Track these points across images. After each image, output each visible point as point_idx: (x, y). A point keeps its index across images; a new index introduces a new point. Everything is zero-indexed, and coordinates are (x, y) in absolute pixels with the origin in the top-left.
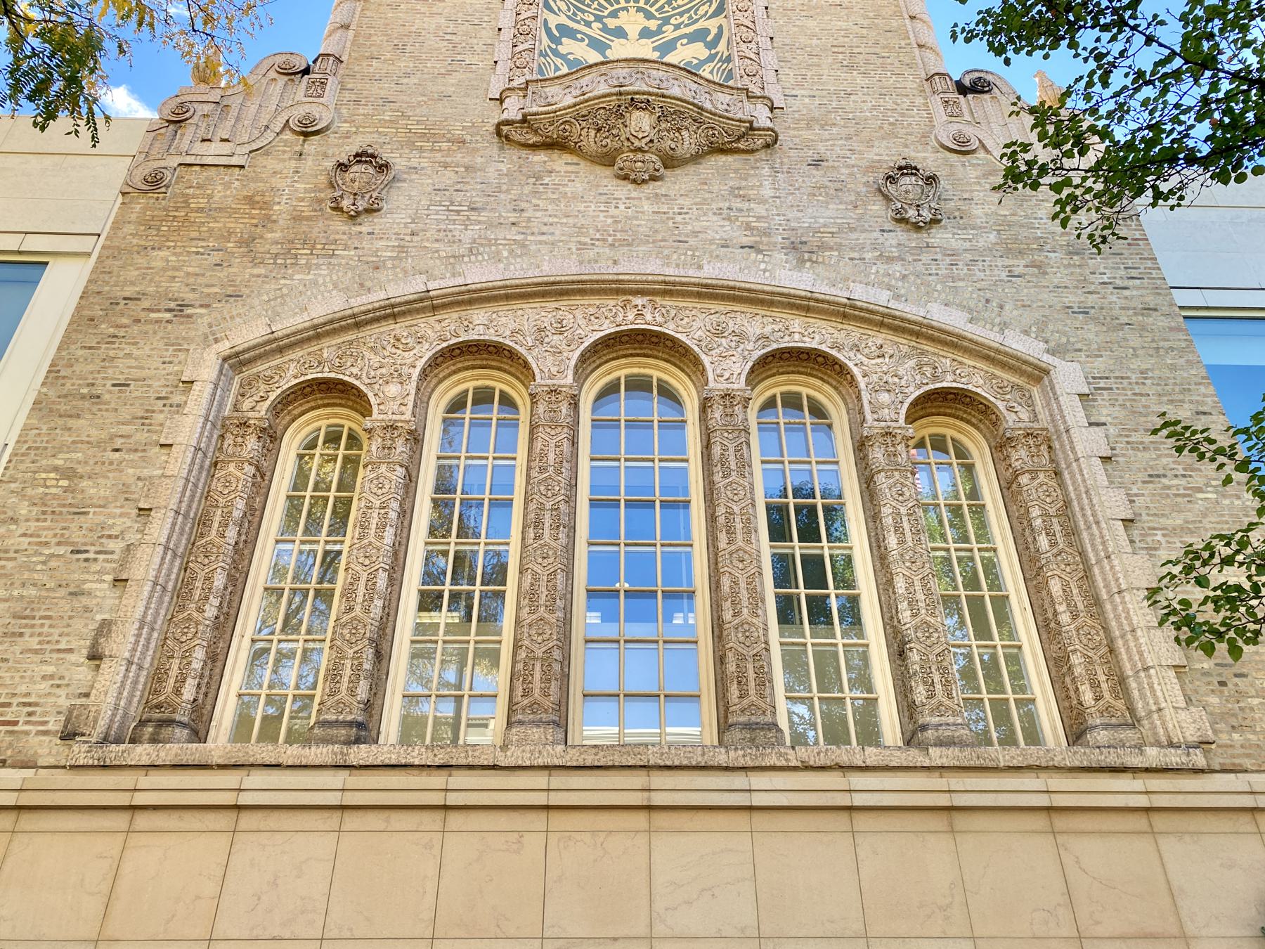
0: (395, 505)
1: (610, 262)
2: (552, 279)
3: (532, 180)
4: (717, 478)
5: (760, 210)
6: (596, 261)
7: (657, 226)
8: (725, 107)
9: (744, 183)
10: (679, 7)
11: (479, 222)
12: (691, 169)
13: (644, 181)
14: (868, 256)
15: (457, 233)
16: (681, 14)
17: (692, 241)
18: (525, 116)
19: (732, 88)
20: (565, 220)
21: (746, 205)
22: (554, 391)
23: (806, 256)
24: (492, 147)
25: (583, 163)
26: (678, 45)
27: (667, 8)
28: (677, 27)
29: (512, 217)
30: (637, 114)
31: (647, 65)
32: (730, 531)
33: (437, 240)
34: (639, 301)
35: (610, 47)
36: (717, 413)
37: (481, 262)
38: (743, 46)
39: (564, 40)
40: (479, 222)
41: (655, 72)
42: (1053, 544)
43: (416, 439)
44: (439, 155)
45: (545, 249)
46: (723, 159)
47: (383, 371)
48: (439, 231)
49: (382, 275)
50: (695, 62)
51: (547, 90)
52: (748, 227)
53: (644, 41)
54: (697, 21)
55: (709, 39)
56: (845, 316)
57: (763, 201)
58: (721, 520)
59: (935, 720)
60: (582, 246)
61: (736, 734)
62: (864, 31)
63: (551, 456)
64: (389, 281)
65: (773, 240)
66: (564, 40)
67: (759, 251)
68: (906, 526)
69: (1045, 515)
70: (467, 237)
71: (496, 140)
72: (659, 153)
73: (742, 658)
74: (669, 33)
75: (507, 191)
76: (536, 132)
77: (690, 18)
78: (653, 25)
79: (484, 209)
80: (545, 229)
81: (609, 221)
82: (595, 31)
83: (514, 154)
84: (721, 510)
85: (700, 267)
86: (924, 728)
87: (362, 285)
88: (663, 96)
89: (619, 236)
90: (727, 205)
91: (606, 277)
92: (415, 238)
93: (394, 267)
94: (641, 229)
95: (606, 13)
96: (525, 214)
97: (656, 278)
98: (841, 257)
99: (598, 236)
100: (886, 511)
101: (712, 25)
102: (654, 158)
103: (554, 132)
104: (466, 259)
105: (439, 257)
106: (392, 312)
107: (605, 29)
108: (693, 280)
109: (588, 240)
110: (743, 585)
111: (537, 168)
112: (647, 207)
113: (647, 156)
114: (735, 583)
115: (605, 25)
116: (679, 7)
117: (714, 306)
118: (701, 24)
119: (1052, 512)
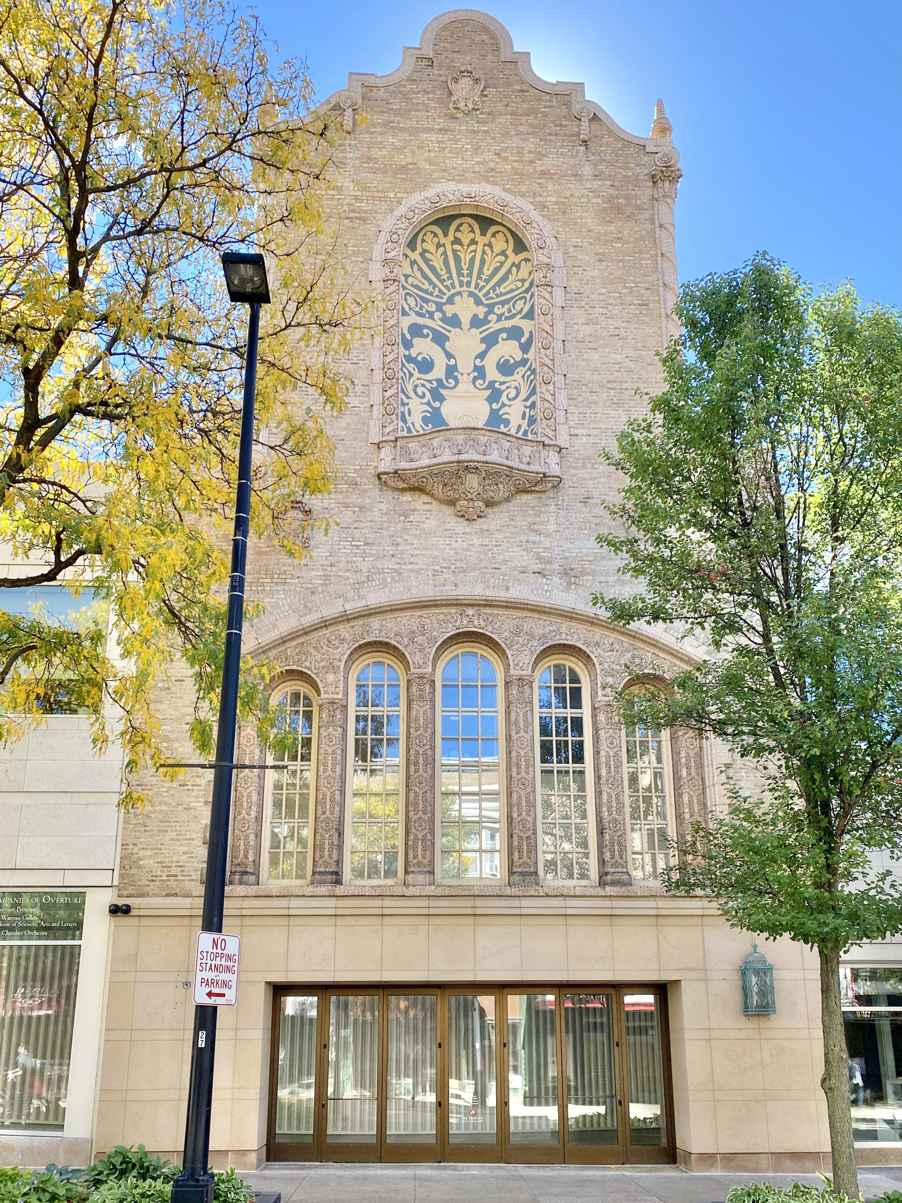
0: (339, 752)
3: (403, 518)
4: (513, 733)
5: (546, 542)
8: (528, 459)
10: (502, 294)
11: (372, 555)
12: (504, 506)
14: (610, 579)
16: (503, 303)
21: (536, 538)
22: (421, 677)
23: (573, 580)
25: (434, 502)
27: (492, 295)
29: (391, 550)
32: (518, 766)
34: (470, 611)
35: (448, 339)
36: (514, 691)
38: (544, 387)
39: (416, 341)
40: (372, 555)
42: (689, 774)
43: (345, 707)
44: (341, 496)
45: (413, 576)
46: (525, 497)
47: (323, 663)
49: (317, 598)
50: (512, 361)
52: (539, 557)
54: (514, 316)
55: (523, 340)
56: (592, 623)
58: (514, 759)
59: (613, 870)
60: (436, 573)
61: (516, 878)
62: (632, 365)
63: (421, 720)
64: (322, 603)
66: (416, 341)
67: (544, 576)
68: (612, 763)
69: (688, 756)
70: (365, 567)
72: (483, 500)
73: (521, 838)
74: (494, 326)
77: (509, 310)
78: (481, 311)
80: (412, 559)
81: (452, 552)
82: (436, 324)
83: (389, 495)
84: (514, 754)
85: (507, 589)
86: (607, 874)
87: (306, 606)
92: (334, 569)
93: (323, 592)
94: (472, 559)
100: (603, 753)
101: (526, 326)
102: (481, 504)
106: (325, 624)
107: (444, 319)
109: (438, 568)
110: (523, 798)
112: (476, 541)
114: (519, 797)
115: (444, 313)
116: (502, 294)
117: (515, 613)
118: (517, 322)
119: (692, 755)
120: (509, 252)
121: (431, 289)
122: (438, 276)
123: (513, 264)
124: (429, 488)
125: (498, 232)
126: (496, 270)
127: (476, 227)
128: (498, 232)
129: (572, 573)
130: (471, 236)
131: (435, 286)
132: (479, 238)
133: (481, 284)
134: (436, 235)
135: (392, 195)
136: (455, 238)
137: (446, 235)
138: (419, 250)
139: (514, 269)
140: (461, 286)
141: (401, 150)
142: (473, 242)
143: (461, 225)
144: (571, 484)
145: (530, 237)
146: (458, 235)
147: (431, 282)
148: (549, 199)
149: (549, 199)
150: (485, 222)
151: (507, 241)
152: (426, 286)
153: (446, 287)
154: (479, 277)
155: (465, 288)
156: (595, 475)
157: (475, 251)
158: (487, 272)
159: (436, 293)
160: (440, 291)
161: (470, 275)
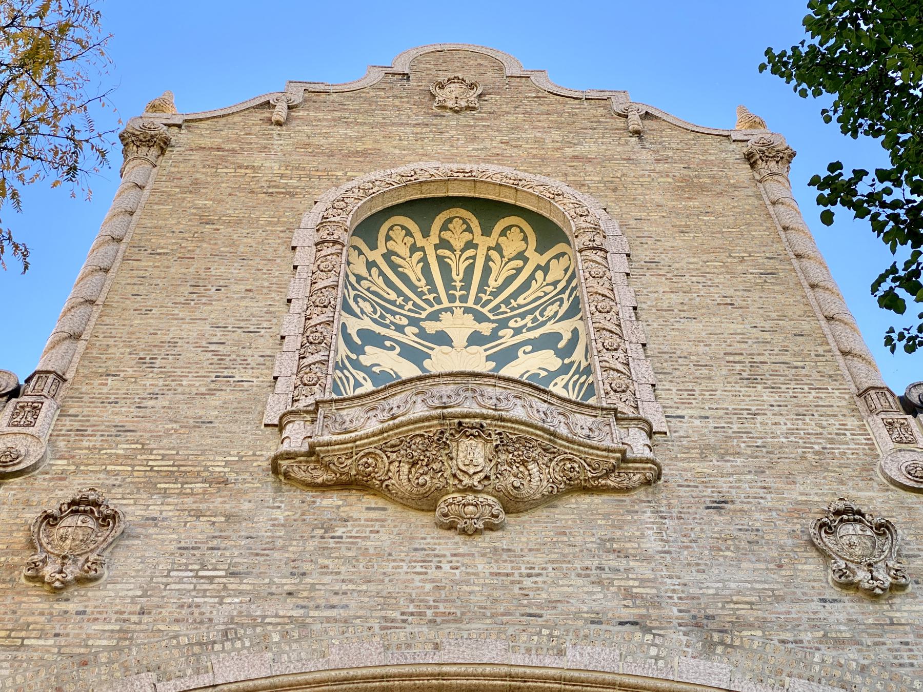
1: (431, 646)
2: (343, 673)
5: (644, 570)
6: (409, 646)
7: (496, 594)
8: (586, 432)
9: (618, 533)
10: (520, 306)
11: (241, 593)
12: (542, 513)
13: (477, 531)
14: (807, 637)
15: (206, 609)
16: (523, 316)
17: (548, 615)
18: (312, 447)
19: (595, 408)
20: (364, 587)
21: (622, 564)
23: (716, 637)
24: (262, 488)
25: (391, 508)
26: (520, 353)
27: (503, 308)
28: (518, 331)
29: (289, 584)
30: (466, 442)
31: (479, 381)
33: (177, 621)
35: (429, 356)
37: (239, 651)
38: (607, 356)
40: (241, 593)
41: (490, 389)
45: (334, 630)
46: (586, 501)
48: (182, 606)
51: (344, 412)
53: (474, 349)
55: (560, 345)
57: (646, 558)
60: (388, 624)
64: (101, 683)
65: (665, 612)
67: (647, 630)
70: (220, 616)
71: (271, 478)
74: (507, 338)
75: (283, 548)
76: (327, 467)
77: (535, 320)
78: (486, 329)
79: (248, 574)
80: (335, 600)
81: (428, 587)
82: (410, 336)
83: (296, 496)
85: (561, 653)
88: (502, 419)
89: (442, 610)
90: (596, 563)
91: (424, 669)
92: (145, 619)
93: (110, 662)
95: (424, 315)
96: (307, 580)
97: (496, 670)
98: (767, 639)
99: (412, 609)
101: (565, 329)
102: (491, 499)
103: (351, 467)
104: (218, 647)
105: (178, 645)
107: (422, 334)
108: (551, 672)
109: (396, 615)
111: (327, 515)
112: (481, 566)
113: (481, 498)
115: (422, 330)
116: (520, 306)
120: (530, 253)
121: (400, 300)
122: (413, 288)
123: (538, 267)
124: (381, 475)
125: (509, 228)
126: (509, 280)
127: (475, 223)
128: (509, 228)
129: (713, 625)
130: (467, 236)
131: (407, 299)
132: (478, 239)
133: (485, 298)
134: (409, 233)
135: (340, 174)
136: (441, 239)
137: (426, 234)
138: (382, 249)
139: (539, 275)
140: (452, 299)
141: (360, 139)
142: (470, 245)
143: (450, 220)
144: (681, 482)
145: (562, 212)
146: (446, 235)
147: (400, 293)
148: (587, 178)
149: (587, 178)
150: (488, 210)
151: (525, 239)
152: (393, 296)
153: (427, 301)
154: (481, 289)
155: (458, 303)
156: (731, 470)
157: (474, 257)
158: (493, 283)
159: (410, 305)
160: (415, 304)
161: (467, 287)
